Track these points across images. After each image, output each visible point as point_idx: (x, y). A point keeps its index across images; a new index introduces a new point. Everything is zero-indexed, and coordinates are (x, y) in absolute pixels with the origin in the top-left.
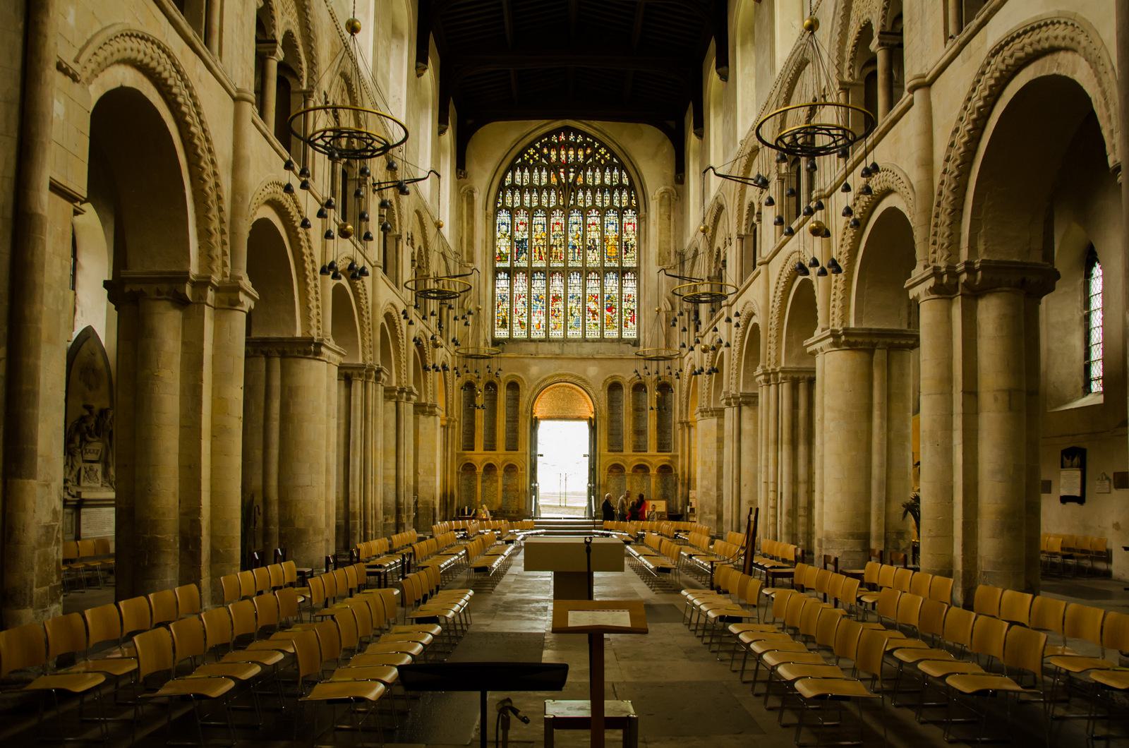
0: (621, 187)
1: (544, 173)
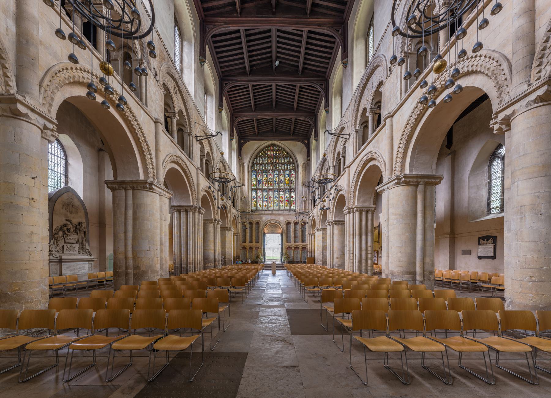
0: (290, 163)
1: (266, 159)
